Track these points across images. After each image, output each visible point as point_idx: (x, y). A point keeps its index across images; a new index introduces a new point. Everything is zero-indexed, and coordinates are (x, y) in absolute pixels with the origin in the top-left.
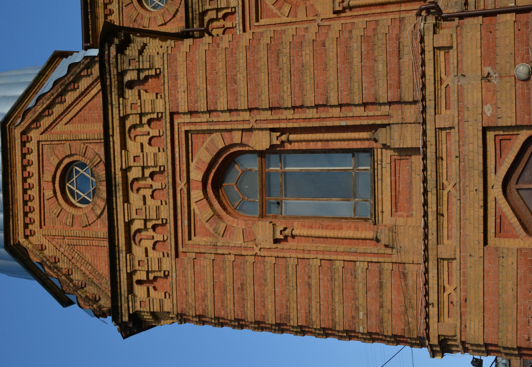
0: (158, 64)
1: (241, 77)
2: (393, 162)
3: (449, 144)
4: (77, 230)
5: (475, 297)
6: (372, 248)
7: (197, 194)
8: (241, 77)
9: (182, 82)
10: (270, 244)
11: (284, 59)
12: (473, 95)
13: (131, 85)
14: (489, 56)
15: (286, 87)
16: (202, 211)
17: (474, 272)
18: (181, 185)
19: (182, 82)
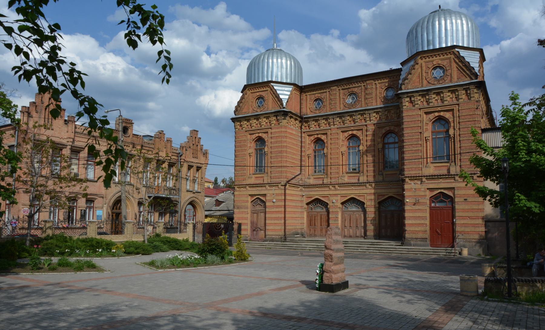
0: (281, 124)
1: (277, 145)
2: (263, 177)
3: (264, 188)
4: (250, 103)
5: (241, 193)
6: (248, 174)
7: (257, 135)
8: (277, 145)
9: (277, 130)
10: (248, 152)
11: (279, 154)
12: (271, 192)
13: (277, 118)
14: (277, 195)
15: (274, 155)
16: (254, 136)
17: (245, 193)
18: (258, 131)
19: (277, 130)
